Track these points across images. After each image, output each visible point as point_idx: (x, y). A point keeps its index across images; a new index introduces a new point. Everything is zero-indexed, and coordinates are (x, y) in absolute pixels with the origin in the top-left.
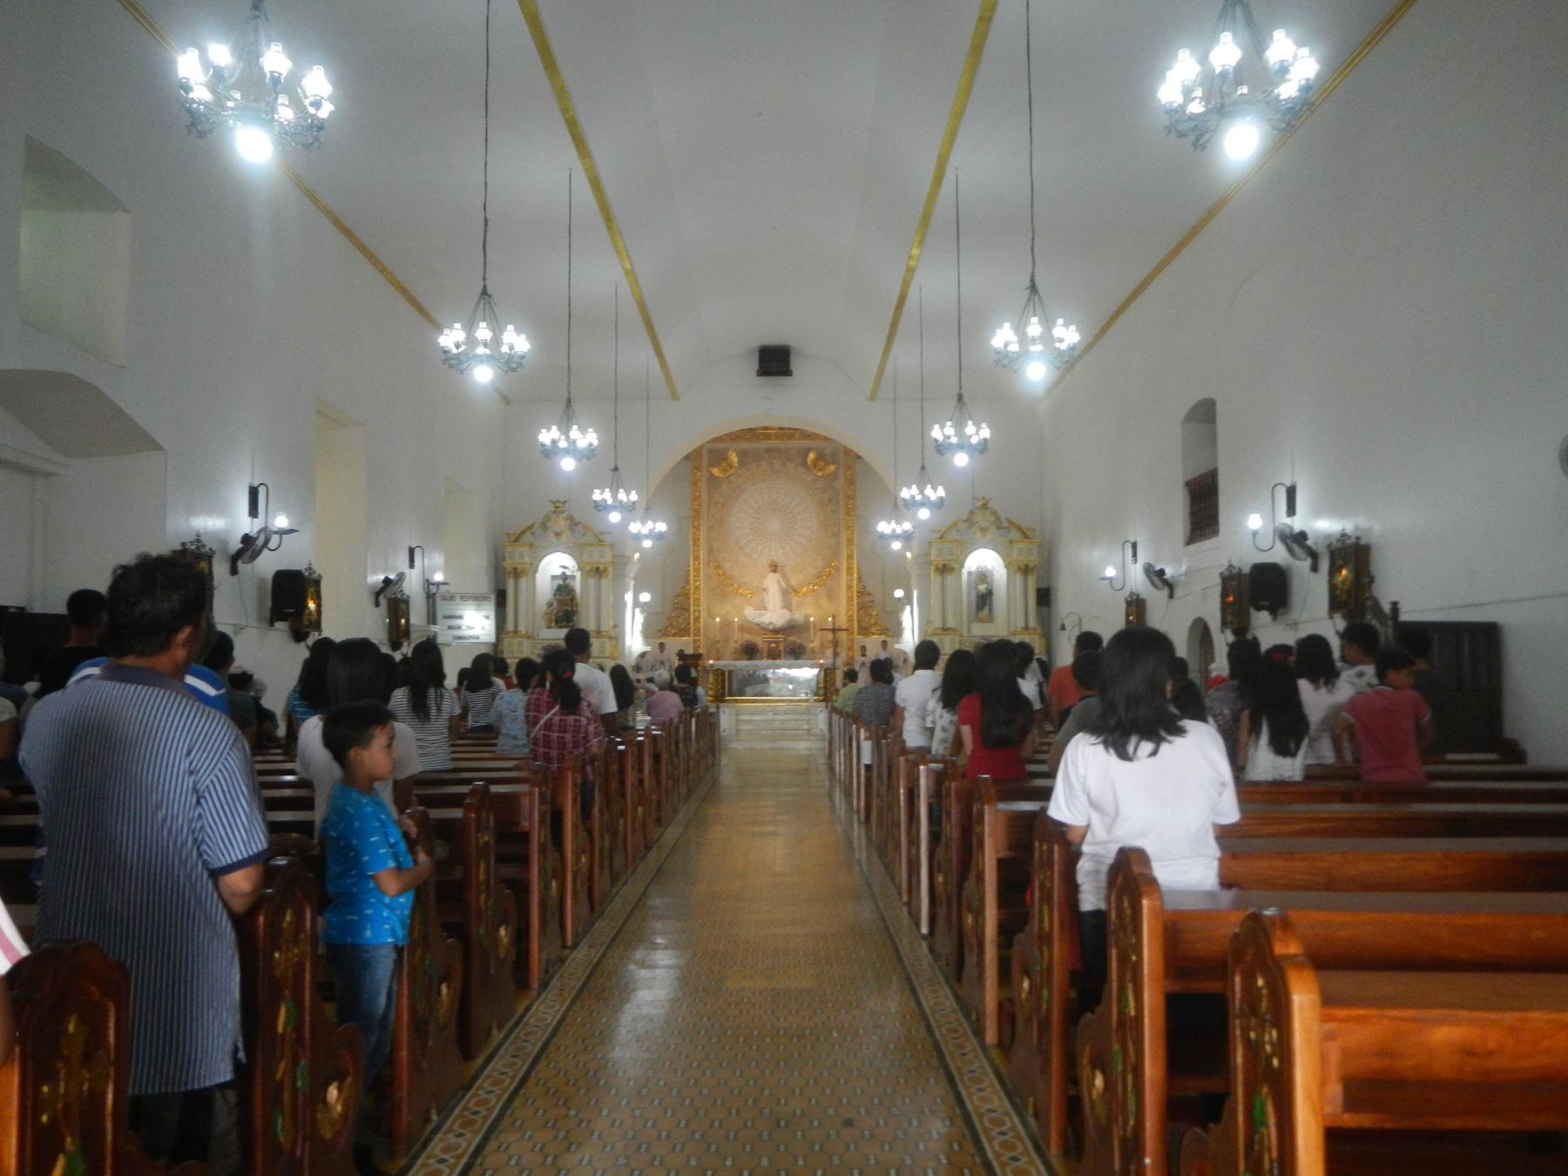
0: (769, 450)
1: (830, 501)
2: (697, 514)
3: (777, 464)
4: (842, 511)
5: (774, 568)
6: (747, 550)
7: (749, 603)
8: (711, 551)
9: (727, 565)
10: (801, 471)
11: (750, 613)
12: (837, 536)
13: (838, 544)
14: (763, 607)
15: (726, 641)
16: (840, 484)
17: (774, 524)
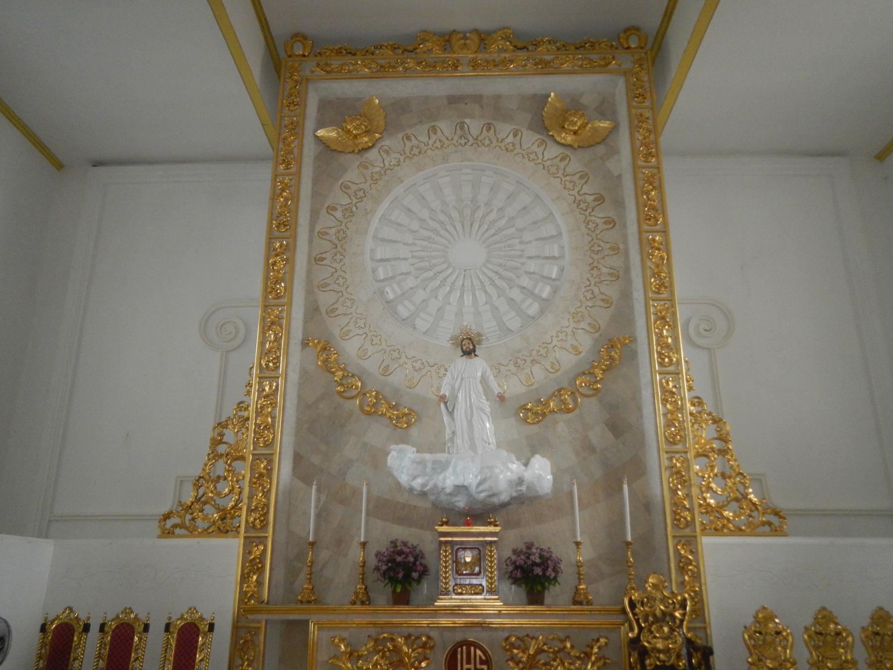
0: (453, 100)
1: (600, 199)
2: (281, 224)
3: (474, 126)
4: (631, 215)
5: (468, 347)
6: (403, 311)
7: (404, 440)
8: (313, 311)
9: (351, 348)
10: (530, 138)
11: (405, 464)
12: (621, 276)
13: (626, 295)
14: (437, 444)
15: (340, 542)
16: (622, 162)
17: (469, 252)
